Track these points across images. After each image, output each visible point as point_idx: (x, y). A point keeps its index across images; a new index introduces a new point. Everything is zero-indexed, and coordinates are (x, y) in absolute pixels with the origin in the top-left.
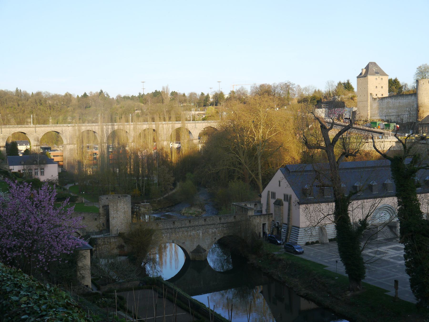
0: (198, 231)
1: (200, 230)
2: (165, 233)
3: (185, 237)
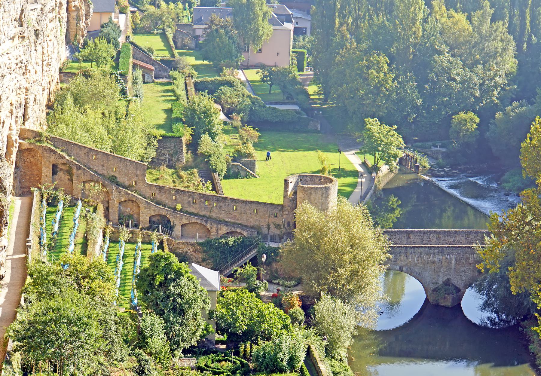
0: (448, 255)
1: (453, 254)
3: (423, 264)
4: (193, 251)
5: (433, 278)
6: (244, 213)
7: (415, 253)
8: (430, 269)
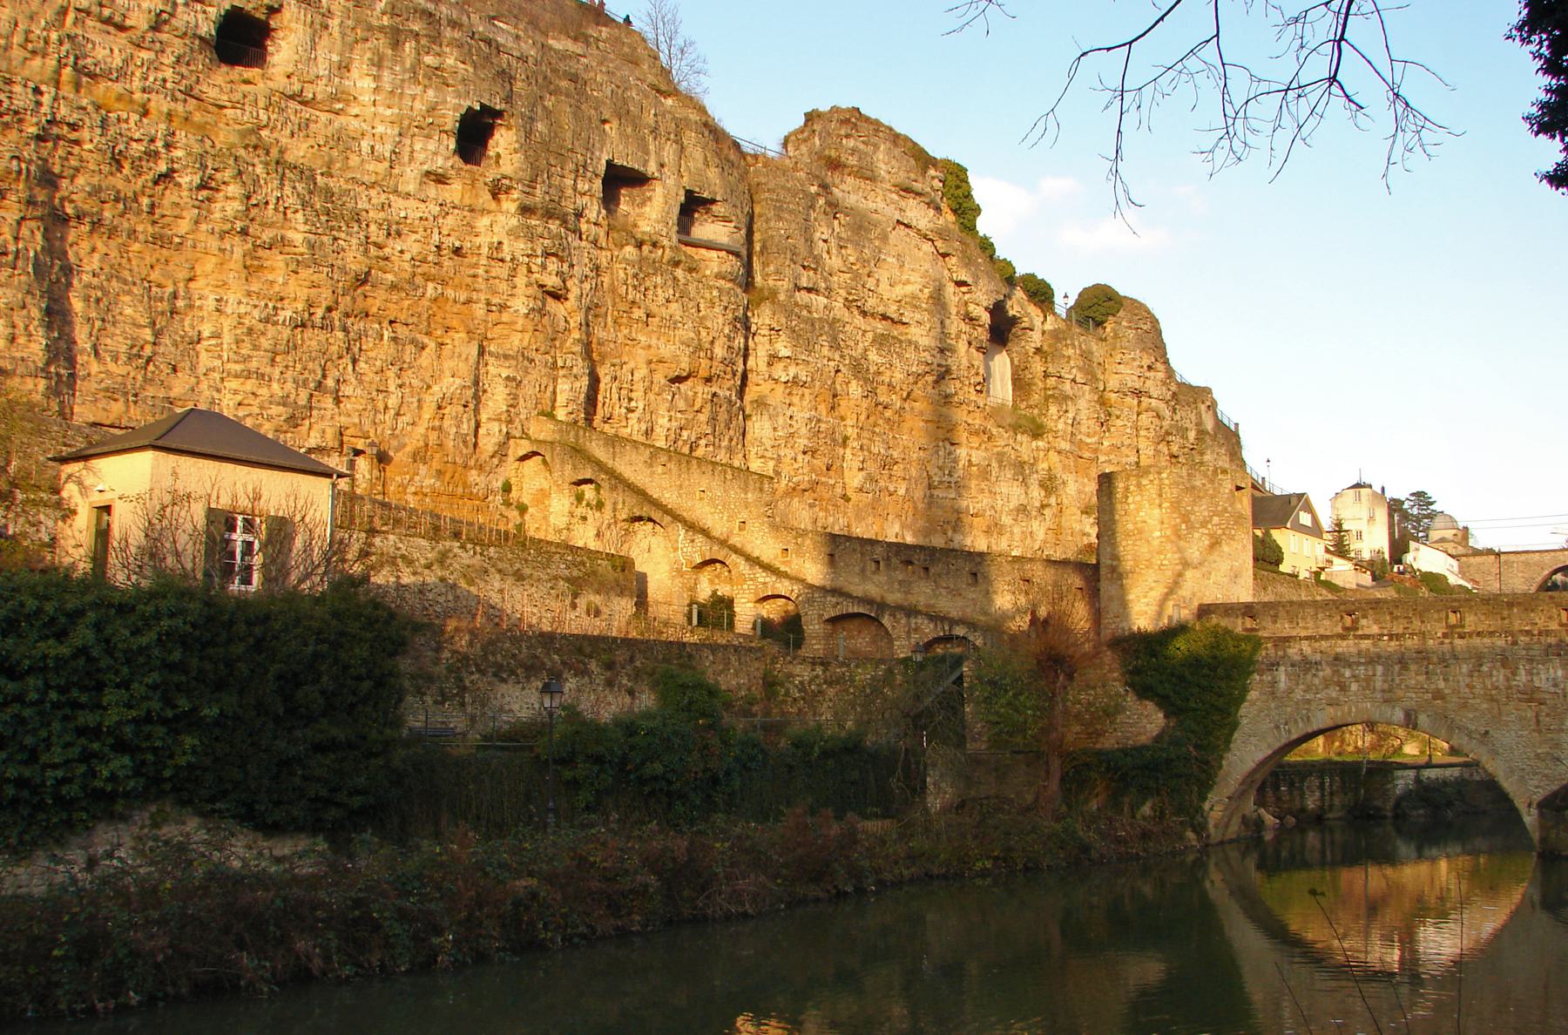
2: (1359, 664)
3: (1492, 699)
5: (1538, 756)
8: (1521, 719)
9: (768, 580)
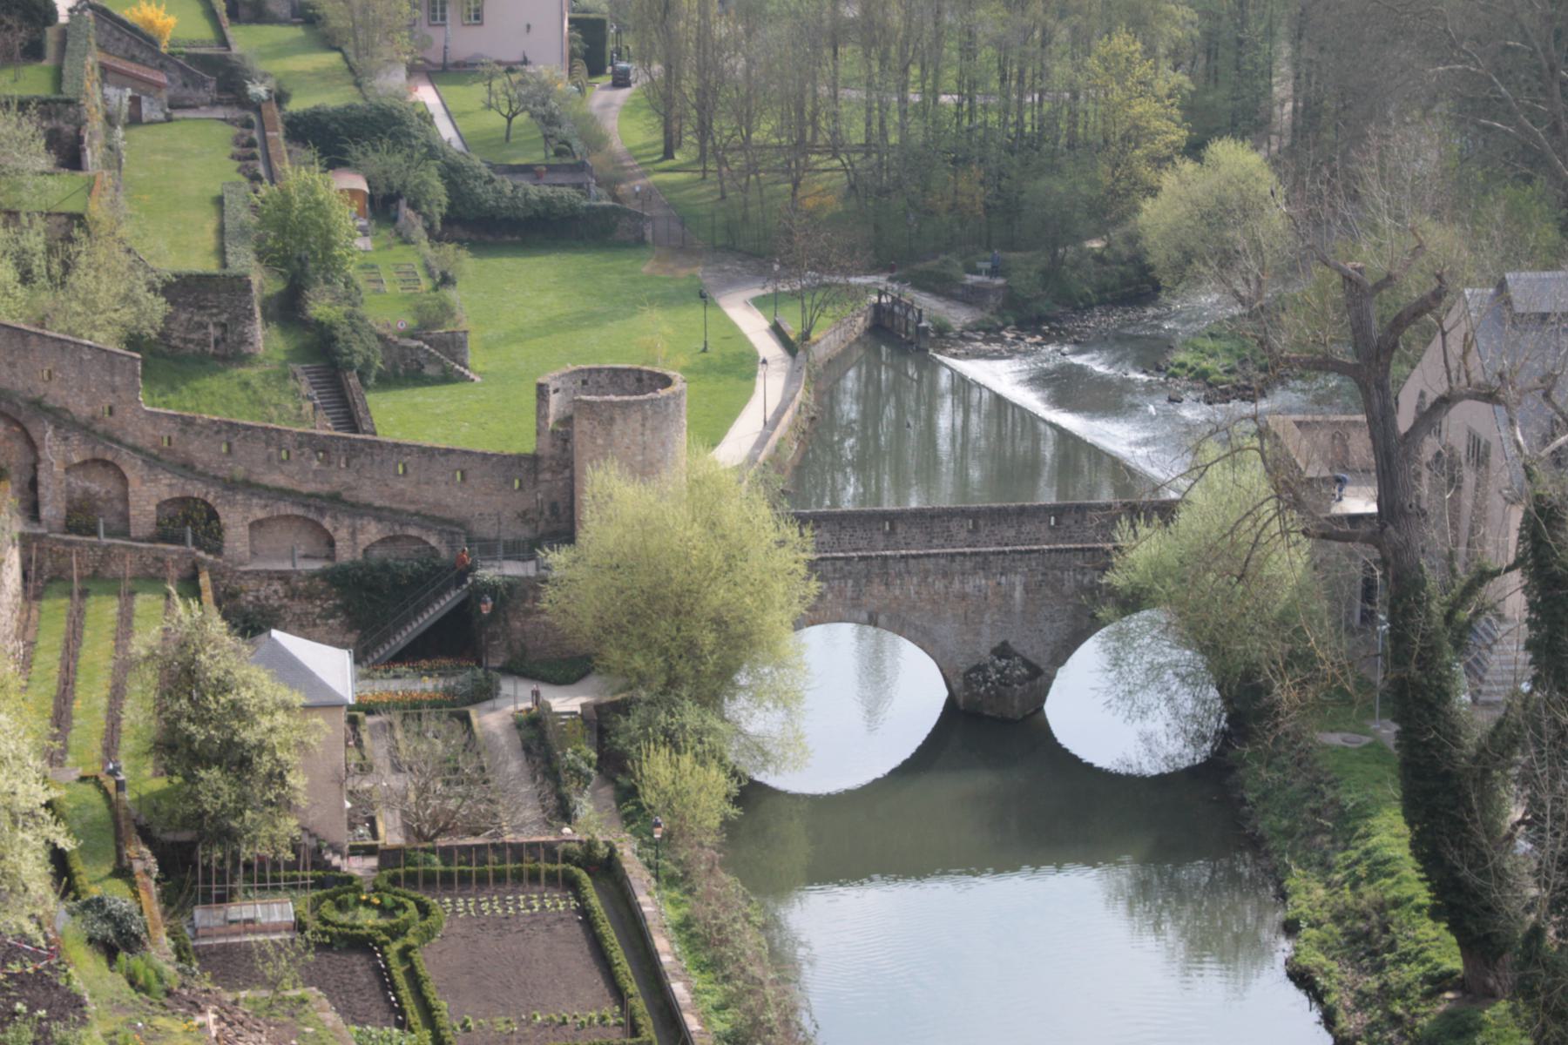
0: (1002, 574)
1: (1016, 573)
2: (834, 579)
3: (935, 602)
4: (286, 596)
5: (964, 642)
6: (427, 483)
7: (909, 572)
8: (954, 615)
9: (174, 481)
